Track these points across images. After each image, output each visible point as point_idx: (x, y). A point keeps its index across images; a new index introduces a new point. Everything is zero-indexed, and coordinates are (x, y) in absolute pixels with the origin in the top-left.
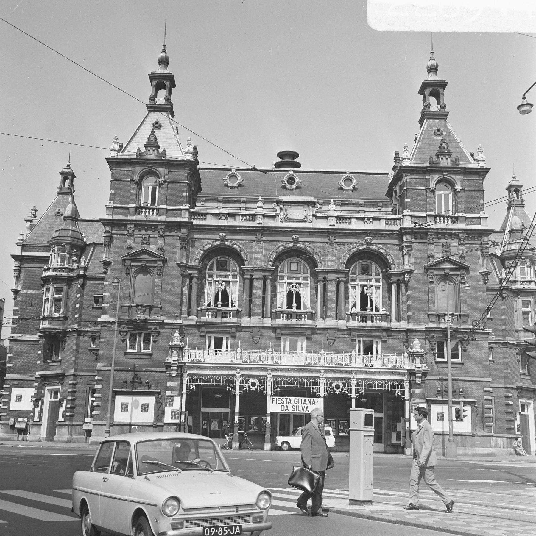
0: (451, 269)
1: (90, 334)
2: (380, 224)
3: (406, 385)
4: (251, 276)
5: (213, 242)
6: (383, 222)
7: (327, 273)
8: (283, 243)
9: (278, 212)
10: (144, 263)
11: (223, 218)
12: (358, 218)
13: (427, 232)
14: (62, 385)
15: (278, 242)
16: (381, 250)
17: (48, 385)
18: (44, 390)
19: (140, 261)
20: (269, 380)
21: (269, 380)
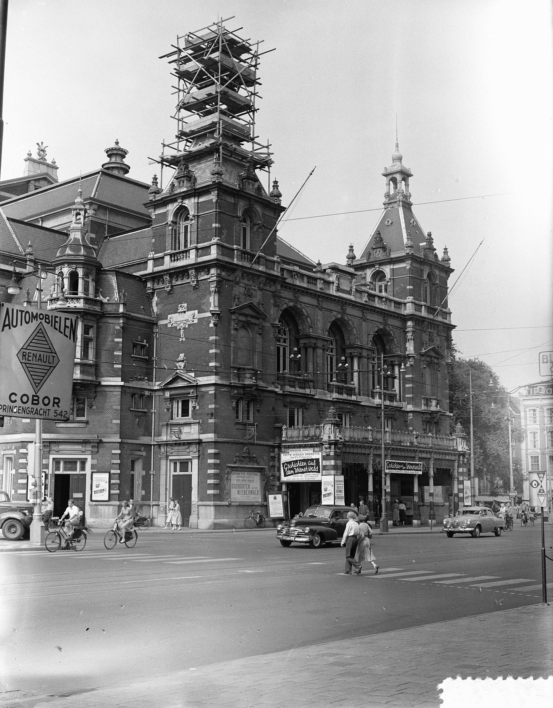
0: (435, 358)
2: (391, 306)
3: (456, 464)
4: (315, 344)
5: (289, 302)
7: (362, 348)
8: (334, 313)
9: (333, 278)
11: (296, 277)
12: (381, 298)
13: (424, 321)
14: (92, 453)
15: (331, 311)
16: (391, 332)
17: (57, 452)
19: (246, 315)
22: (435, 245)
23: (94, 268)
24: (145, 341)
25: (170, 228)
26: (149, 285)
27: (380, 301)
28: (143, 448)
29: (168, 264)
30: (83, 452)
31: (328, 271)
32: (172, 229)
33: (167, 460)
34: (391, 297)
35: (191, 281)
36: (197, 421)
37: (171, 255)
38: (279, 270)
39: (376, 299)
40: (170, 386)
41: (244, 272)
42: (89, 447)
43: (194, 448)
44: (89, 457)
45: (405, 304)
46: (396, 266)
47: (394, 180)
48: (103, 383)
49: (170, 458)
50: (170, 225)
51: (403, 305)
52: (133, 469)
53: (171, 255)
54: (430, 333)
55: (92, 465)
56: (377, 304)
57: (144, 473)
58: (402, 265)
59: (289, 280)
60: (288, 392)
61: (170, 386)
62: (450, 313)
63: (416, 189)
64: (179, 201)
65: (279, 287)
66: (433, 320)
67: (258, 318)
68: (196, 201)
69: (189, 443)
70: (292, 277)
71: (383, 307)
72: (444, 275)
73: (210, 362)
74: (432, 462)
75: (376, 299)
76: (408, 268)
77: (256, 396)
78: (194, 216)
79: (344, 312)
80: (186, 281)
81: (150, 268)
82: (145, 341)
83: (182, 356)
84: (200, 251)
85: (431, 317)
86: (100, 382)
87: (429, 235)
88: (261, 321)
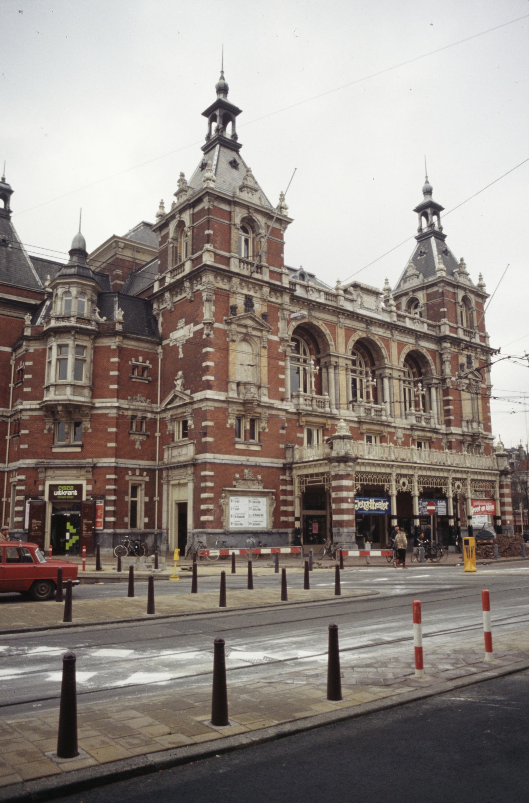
1: (130, 413)
2: (423, 328)
3: (497, 485)
4: (336, 362)
6: (425, 325)
10: (250, 330)
11: (311, 292)
17: (53, 478)
18: (44, 484)
19: (246, 326)
20: (416, 479)
21: (416, 479)
22: (468, 270)
23: (90, 288)
24: (148, 362)
25: (171, 245)
26: (155, 306)
27: (411, 322)
28: (145, 474)
29: (169, 280)
30: (78, 477)
31: (351, 289)
32: (173, 247)
33: (168, 485)
34: (422, 319)
35: (187, 294)
36: (192, 441)
37: (171, 272)
38: (287, 282)
39: (407, 319)
40: (169, 407)
42: (83, 472)
43: (190, 471)
44: (84, 483)
45: (439, 326)
46: (430, 291)
47: (426, 215)
48: (97, 405)
49: (172, 482)
50: (171, 243)
51: (437, 328)
52: (134, 495)
53: (171, 272)
54: (467, 355)
55: (87, 491)
56: (408, 324)
57: (147, 499)
58: (435, 289)
59: (299, 292)
60: (303, 410)
61: (169, 407)
62: (488, 337)
63: (447, 222)
64: (177, 216)
65: (286, 299)
66: (470, 342)
67: (261, 331)
68: (191, 212)
69: (184, 466)
70: (307, 291)
71: (413, 327)
72: (480, 301)
73: (203, 376)
74: (469, 482)
75: (407, 319)
76: (440, 291)
77: (260, 413)
78: (189, 228)
79: (368, 331)
80: (184, 295)
81: (156, 288)
82: (148, 362)
83: (180, 373)
84: (195, 262)
85: (467, 339)
86: (94, 404)
87: (462, 260)
88: (265, 333)
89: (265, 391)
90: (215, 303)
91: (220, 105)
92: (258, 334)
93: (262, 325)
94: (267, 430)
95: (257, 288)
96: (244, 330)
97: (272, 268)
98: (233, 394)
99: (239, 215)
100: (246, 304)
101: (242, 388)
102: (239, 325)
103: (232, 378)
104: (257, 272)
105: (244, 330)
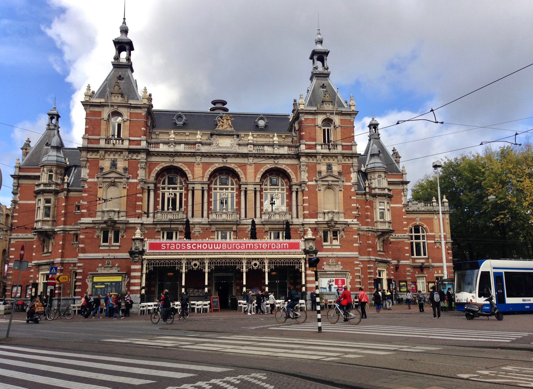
10: (330, 183)
19: (328, 181)
41: (323, 157)
89: (342, 215)
90: (308, 172)
91: (314, 53)
92: (337, 183)
93: (337, 178)
94: (344, 237)
95: (334, 158)
96: (326, 183)
97: (344, 144)
98: (320, 219)
99: (320, 119)
100: (328, 169)
101: (326, 215)
102: (322, 181)
103: (319, 211)
104: (334, 149)
105: (326, 183)
